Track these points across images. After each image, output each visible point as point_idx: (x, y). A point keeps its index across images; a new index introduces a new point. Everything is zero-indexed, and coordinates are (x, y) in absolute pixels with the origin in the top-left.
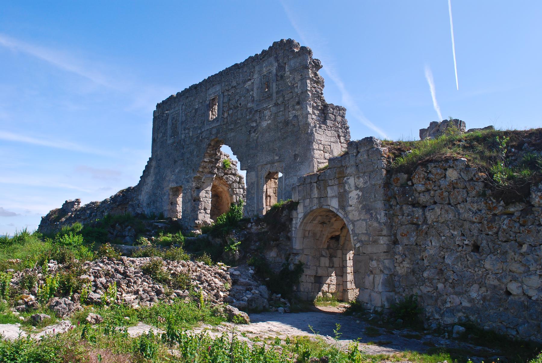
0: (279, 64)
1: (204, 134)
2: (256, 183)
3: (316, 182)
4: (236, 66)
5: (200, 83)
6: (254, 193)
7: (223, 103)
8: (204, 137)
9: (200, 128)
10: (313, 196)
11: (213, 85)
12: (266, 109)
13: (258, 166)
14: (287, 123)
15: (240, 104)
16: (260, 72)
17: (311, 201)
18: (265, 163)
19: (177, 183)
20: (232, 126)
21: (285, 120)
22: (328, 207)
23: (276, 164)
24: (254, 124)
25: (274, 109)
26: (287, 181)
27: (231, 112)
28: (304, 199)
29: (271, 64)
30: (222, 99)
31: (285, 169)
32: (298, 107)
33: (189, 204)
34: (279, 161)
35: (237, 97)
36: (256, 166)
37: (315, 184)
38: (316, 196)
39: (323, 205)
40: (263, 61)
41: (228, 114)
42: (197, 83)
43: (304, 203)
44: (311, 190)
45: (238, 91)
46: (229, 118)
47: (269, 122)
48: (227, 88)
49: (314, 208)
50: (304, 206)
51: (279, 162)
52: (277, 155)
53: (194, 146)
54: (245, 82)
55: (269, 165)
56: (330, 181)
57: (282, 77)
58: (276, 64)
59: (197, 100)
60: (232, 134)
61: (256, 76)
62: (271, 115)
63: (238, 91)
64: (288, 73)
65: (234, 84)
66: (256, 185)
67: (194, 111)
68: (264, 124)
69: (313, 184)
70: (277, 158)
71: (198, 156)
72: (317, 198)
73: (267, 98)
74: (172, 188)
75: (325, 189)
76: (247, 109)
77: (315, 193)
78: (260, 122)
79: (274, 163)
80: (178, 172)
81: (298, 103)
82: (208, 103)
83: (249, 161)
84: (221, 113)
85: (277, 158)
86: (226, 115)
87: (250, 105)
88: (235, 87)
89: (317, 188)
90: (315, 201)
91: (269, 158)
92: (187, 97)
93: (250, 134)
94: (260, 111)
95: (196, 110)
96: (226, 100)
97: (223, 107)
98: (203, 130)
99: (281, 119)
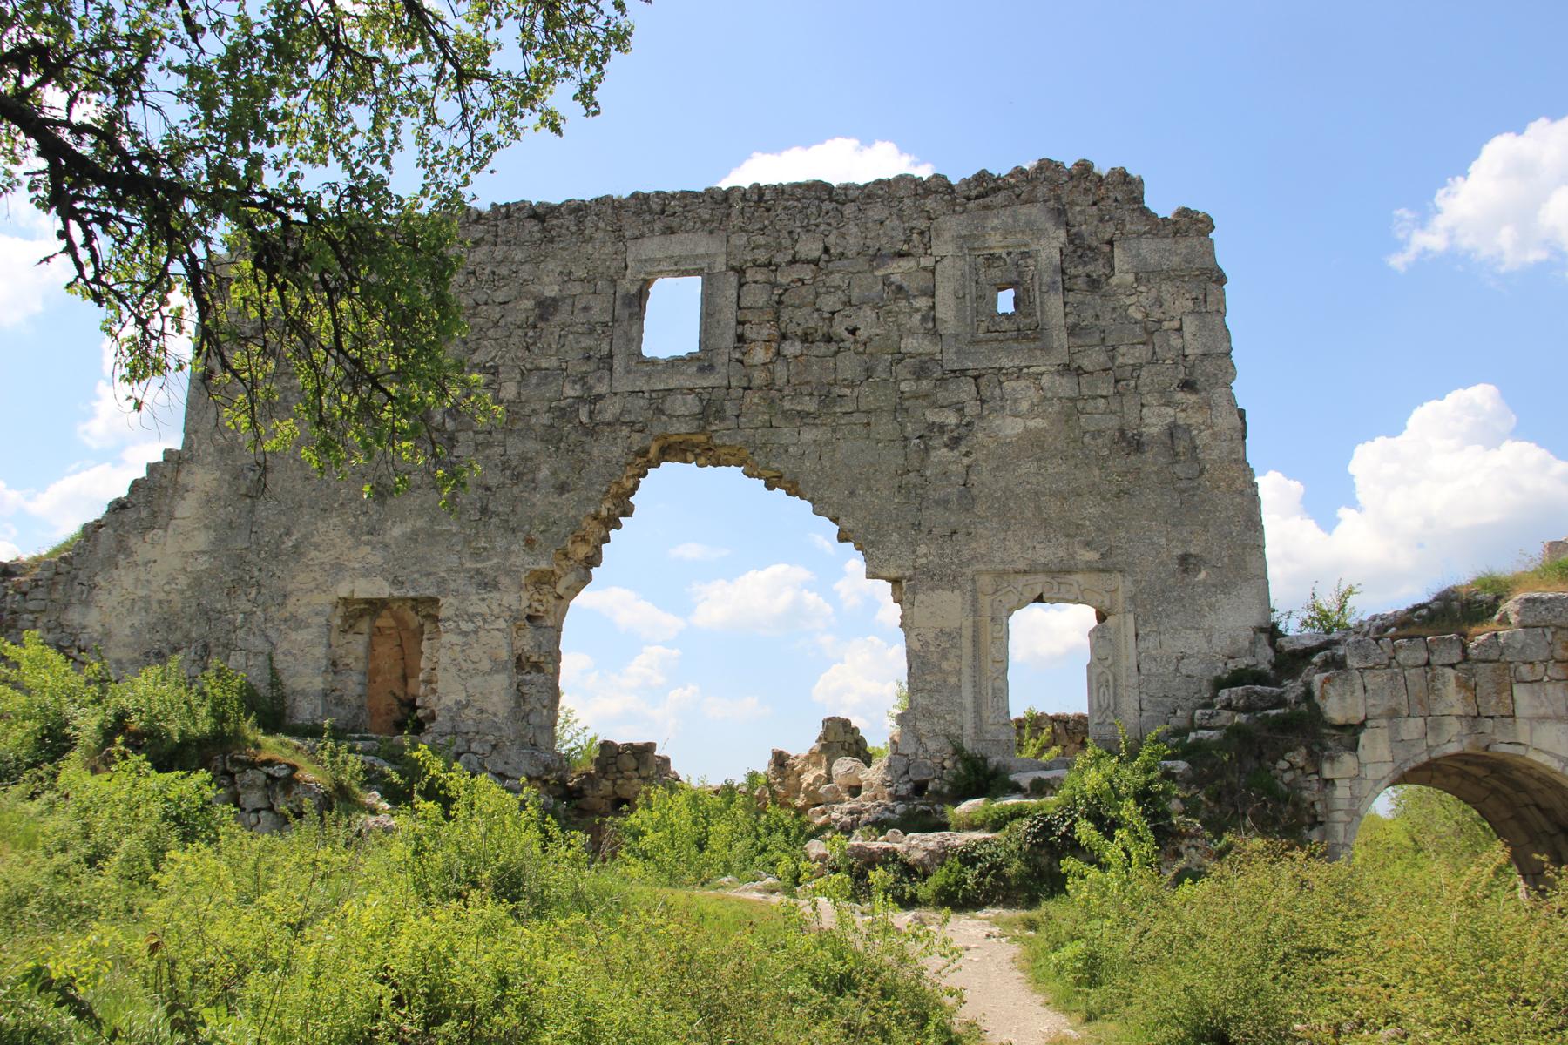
0: (1072, 238)
1: (610, 410)
2: (967, 633)
3: (1452, 666)
4: (819, 190)
5: (577, 210)
6: (959, 672)
7: (739, 308)
8: (608, 417)
9: (582, 379)
10: (1440, 708)
11: (671, 231)
12: (1019, 373)
13: (980, 573)
14: (1133, 443)
15: (853, 331)
16: (966, 242)
17: (1434, 723)
18: (1021, 566)
19: (397, 582)
20: (811, 405)
21: (1122, 432)
22: (1521, 750)
23: (1078, 577)
24: (951, 419)
25: (1065, 386)
26: (1150, 643)
27: (791, 349)
28: (1393, 714)
29: (1039, 233)
30: (732, 293)
31: (1133, 599)
32: (1193, 398)
33: (501, 681)
34: (1103, 569)
35: (829, 302)
36: (969, 571)
37: (1450, 672)
38: (1458, 709)
39: (1494, 742)
40: (987, 207)
41: (778, 353)
42: (556, 200)
43: (1395, 730)
44: (1432, 689)
45: (836, 279)
46: (781, 372)
47: (1036, 423)
48: (762, 256)
49: (1452, 749)
50: (1396, 741)
51: (1103, 571)
52: (1088, 545)
53: (531, 446)
54: (878, 257)
55: (1041, 578)
56: (1524, 669)
57: (1094, 284)
58: (1062, 234)
59: (551, 264)
60: (808, 435)
61: (944, 247)
62: (1044, 399)
63: (836, 279)
64: (1130, 278)
65: (810, 247)
66: (966, 644)
67: (528, 304)
68: (1011, 427)
69: (1439, 670)
70: (1092, 556)
71: (562, 488)
72: (1459, 717)
73: (1016, 339)
74: (346, 601)
75: (1504, 687)
76: (900, 356)
77: (1452, 699)
78: (980, 416)
79: (1069, 572)
80: (413, 537)
81: (1188, 385)
82: (634, 290)
83: (922, 549)
84: (730, 339)
85: (1092, 556)
86: (759, 355)
87: (910, 344)
88: (816, 262)
89: (1462, 684)
90: (1454, 727)
91: (1046, 553)
92: (476, 243)
93: (927, 450)
94: (976, 378)
95: (546, 308)
96: (757, 296)
97: (743, 323)
98: (602, 388)
99: (1099, 418)
